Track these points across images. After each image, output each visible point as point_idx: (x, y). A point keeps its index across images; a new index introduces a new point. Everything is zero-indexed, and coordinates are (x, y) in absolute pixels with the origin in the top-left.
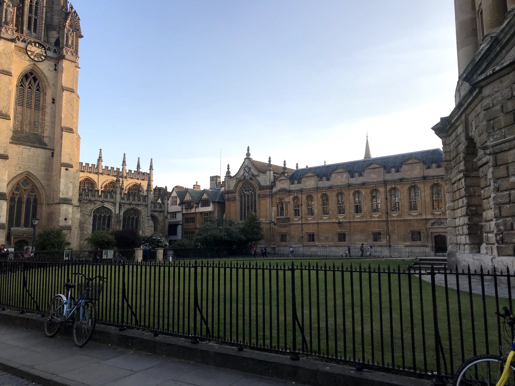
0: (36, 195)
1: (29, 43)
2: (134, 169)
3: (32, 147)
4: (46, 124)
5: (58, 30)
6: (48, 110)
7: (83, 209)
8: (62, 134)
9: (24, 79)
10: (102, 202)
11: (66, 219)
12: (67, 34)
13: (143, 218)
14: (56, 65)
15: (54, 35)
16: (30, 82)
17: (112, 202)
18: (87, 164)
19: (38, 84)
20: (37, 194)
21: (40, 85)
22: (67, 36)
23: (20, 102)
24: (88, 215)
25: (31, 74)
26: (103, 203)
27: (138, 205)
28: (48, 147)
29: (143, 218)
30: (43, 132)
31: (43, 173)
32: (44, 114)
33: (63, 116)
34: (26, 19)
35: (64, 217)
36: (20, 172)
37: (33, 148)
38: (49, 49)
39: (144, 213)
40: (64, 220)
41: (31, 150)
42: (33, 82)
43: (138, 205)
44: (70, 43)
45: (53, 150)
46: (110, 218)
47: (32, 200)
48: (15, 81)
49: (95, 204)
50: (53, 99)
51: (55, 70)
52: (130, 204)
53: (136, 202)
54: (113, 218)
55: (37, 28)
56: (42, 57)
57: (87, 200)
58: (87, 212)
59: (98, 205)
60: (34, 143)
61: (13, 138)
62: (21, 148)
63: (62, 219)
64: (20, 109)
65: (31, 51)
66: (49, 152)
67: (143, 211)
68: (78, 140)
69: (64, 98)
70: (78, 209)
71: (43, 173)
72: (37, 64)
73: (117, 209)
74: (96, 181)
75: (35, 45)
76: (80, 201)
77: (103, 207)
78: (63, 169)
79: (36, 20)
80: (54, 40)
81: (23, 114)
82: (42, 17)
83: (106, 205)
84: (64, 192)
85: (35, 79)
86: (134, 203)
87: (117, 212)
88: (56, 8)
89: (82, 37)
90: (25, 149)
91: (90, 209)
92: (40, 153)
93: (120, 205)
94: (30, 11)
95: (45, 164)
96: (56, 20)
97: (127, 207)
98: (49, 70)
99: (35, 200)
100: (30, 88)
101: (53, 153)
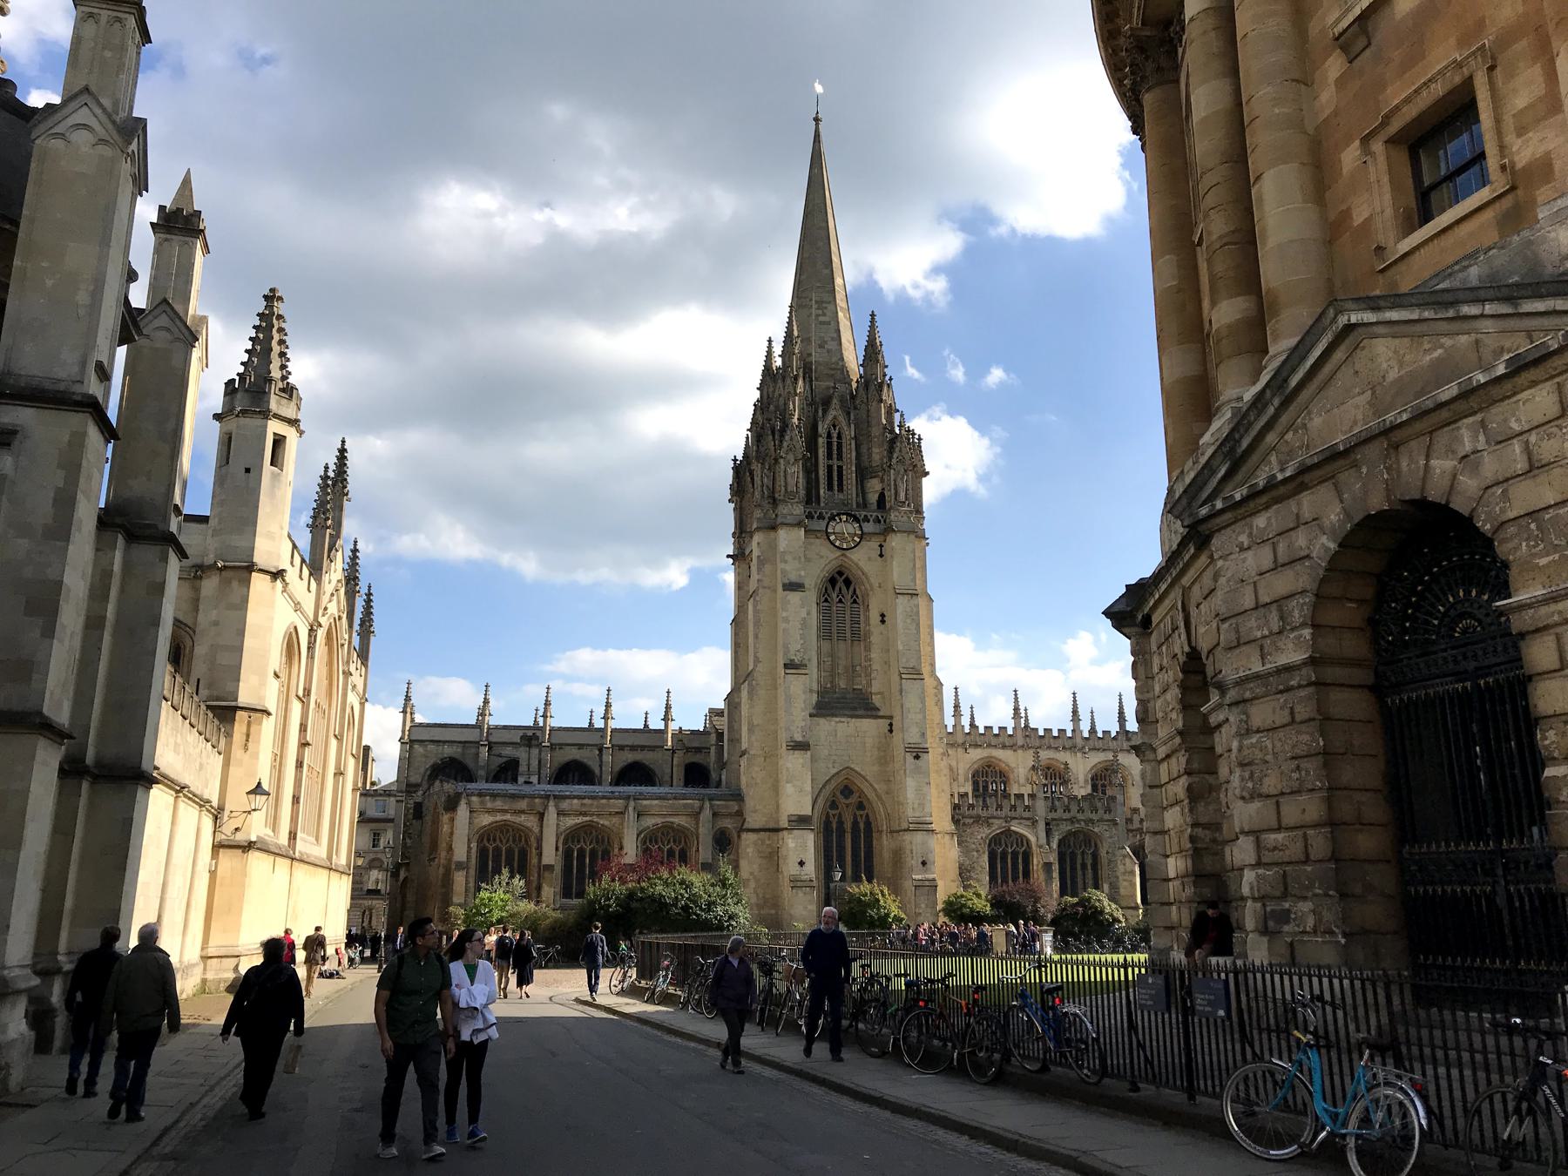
0: (867, 815)
1: (832, 518)
2: (1114, 728)
3: (852, 717)
4: (874, 667)
5: (880, 474)
6: (875, 639)
7: (964, 839)
8: (901, 685)
9: (830, 588)
11: (924, 863)
12: (895, 481)
14: (881, 546)
15: (874, 486)
16: (840, 589)
17: (1028, 819)
19: (855, 590)
20: (870, 815)
21: (858, 592)
22: (895, 485)
23: (827, 631)
24: (978, 851)
25: (840, 573)
28: (881, 713)
30: (870, 684)
31: (876, 768)
32: (868, 649)
33: (900, 648)
34: (822, 472)
35: (920, 860)
36: (834, 771)
38: (866, 520)
39: (1110, 840)
41: (851, 725)
42: (844, 588)
44: (902, 497)
45: (891, 717)
46: (1027, 856)
47: (862, 826)
48: (812, 596)
50: (883, 616)
51: (881, 555)
52: (1072, 820)
54: (1035, 856)
55: (845, 482)
56: (856, 538)
57: (971, 817)
59: (997, 826)
60: (855, 709)
62: (833, 723)
63: (915, 862)
64: (826, 645)
65: (834, 533)
66: (884, 723)
67: (1107, 834)
69: (900, 610)
71: (876, 768)
72: (847, 553)
73: (1043, 834)
74: (1013, 765)
75: (840, 519)
76: (955, 821)
77: (1009, 830)
78: (909, 758)
79: (840, 468)
80: (876, 496)
81: (832, 655)
82: (850, 458)
84: (916, 806)
85: (848, 582)
86: (1080, 816)
87: (1043, 840)
88: (875, 431)
89: (927, 473)
91: (979, 837)
92: (869, 728)
93: (1047, 824)
94: (830, 456)
95: (879, 749)
96: (877, 454)
97: (1066, 827)
98: (870, 559)
99: (868, 824)
100: (840, 601)
101: (891, 725)
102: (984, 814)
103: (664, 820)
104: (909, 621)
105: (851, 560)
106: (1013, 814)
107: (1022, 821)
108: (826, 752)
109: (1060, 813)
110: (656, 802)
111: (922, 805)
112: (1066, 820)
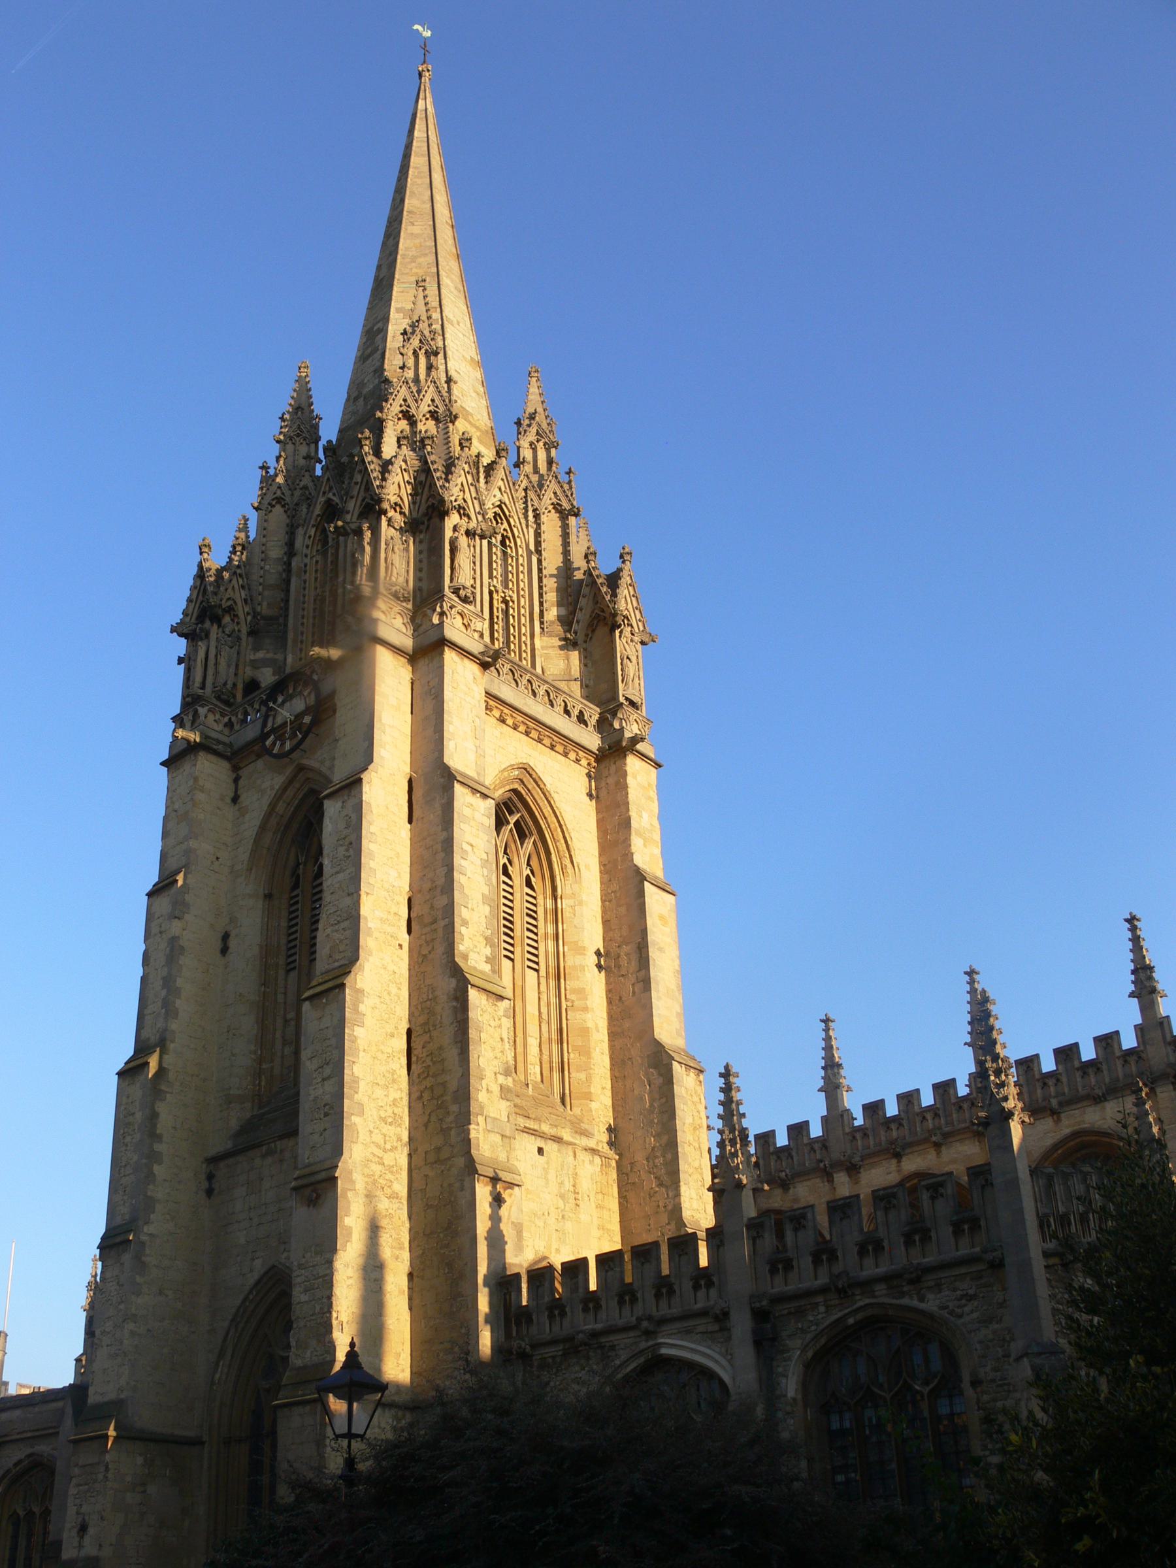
13: (976, 1383)
17: (704, 1313)
18: (1066, 1054)
26: (648, 1334)
27: (916, 1278)
29: (976, 1383)
43: (916, 1278)
52: (842, 1290)
53: (898, 1257)
61: (247, 1128)
73: (745, 1354)
77: (658, 1363)
83: (674, 1346)
86: (871, 1269)
93: (760, 1316)
97: (823, 1317)
103: (29, 1451)
104: (341, 850)
105: (312, 769)
106: (664, 1310)
107: (691, 1323)
109: (806, 1277)
110: (17, 1413)
112: (824, 1290)
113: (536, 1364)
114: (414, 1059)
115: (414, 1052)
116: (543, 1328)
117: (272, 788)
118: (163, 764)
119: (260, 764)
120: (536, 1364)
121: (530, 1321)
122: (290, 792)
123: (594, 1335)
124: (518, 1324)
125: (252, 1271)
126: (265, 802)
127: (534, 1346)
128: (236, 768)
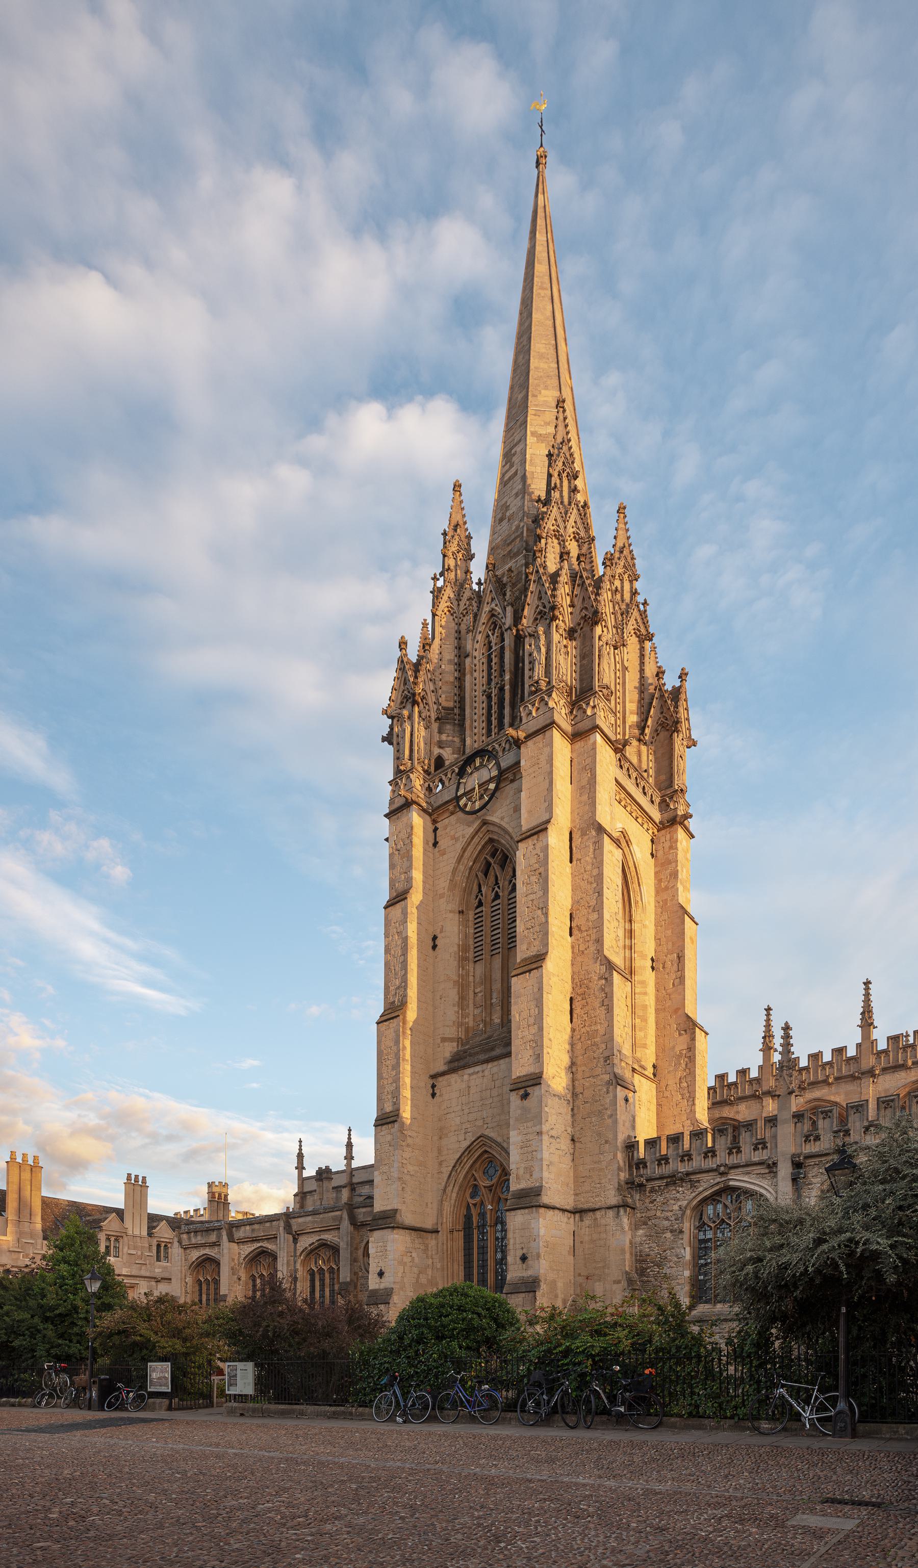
3: (487, 1061)
10: (723, 1171)
36: (467, 1143)
37: (490, 1065)
40: (519, 1261)
41: (486, 1073)
49: (693, 1185)
58: (667, 1219)
62: (466, 1077)
68: (606, 979)
70: (618, 1215)
90: (475, 1076)
91: (676, 1207)
102: (683, 1168)
108: (458, 1120)
111: (529, 1171)
113: (648, 1190)
114: (575, 1016)
115: (575, 1012)
116: (653, 1170)
117: (463, 836)
118: (386, 816)
119: (453, 818)
120: (648, 1190)
121: (645, 1167)
122: (476, 839)
123: (688, 1174)
124: (638, 1168)
125: (465, 1139)
126: (459, 846)
127: (647, 1180)
128: (434, 822)
